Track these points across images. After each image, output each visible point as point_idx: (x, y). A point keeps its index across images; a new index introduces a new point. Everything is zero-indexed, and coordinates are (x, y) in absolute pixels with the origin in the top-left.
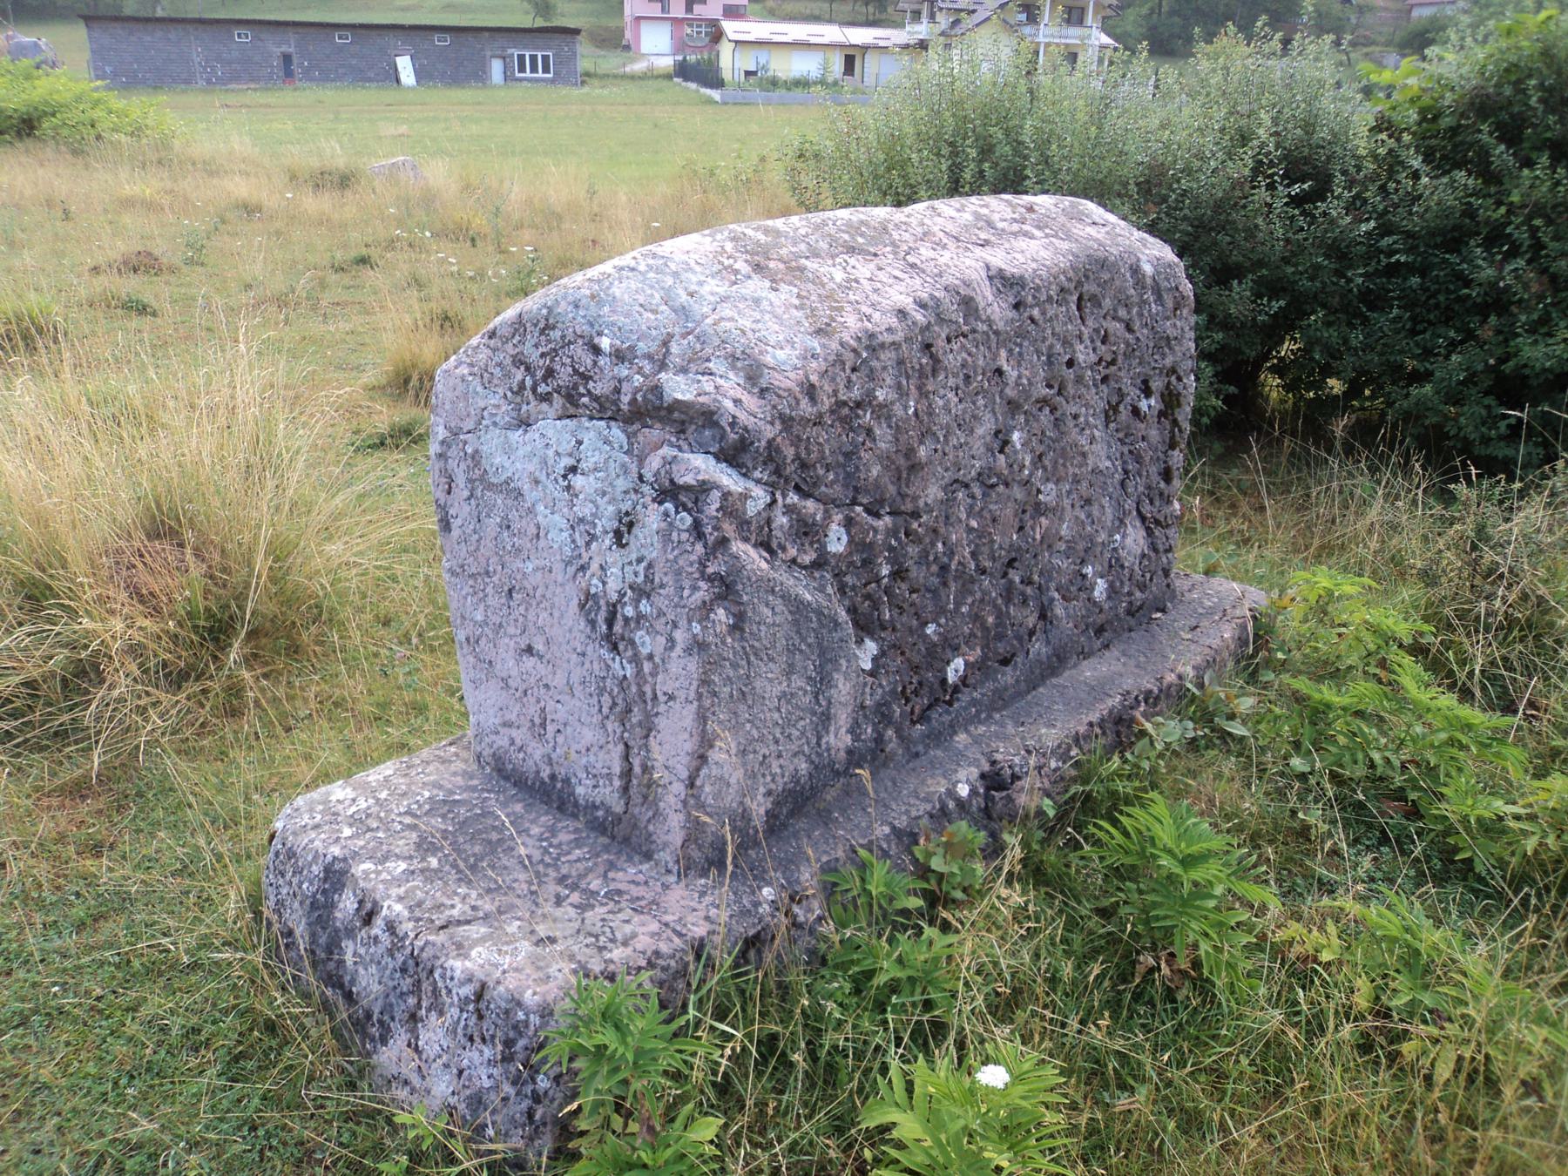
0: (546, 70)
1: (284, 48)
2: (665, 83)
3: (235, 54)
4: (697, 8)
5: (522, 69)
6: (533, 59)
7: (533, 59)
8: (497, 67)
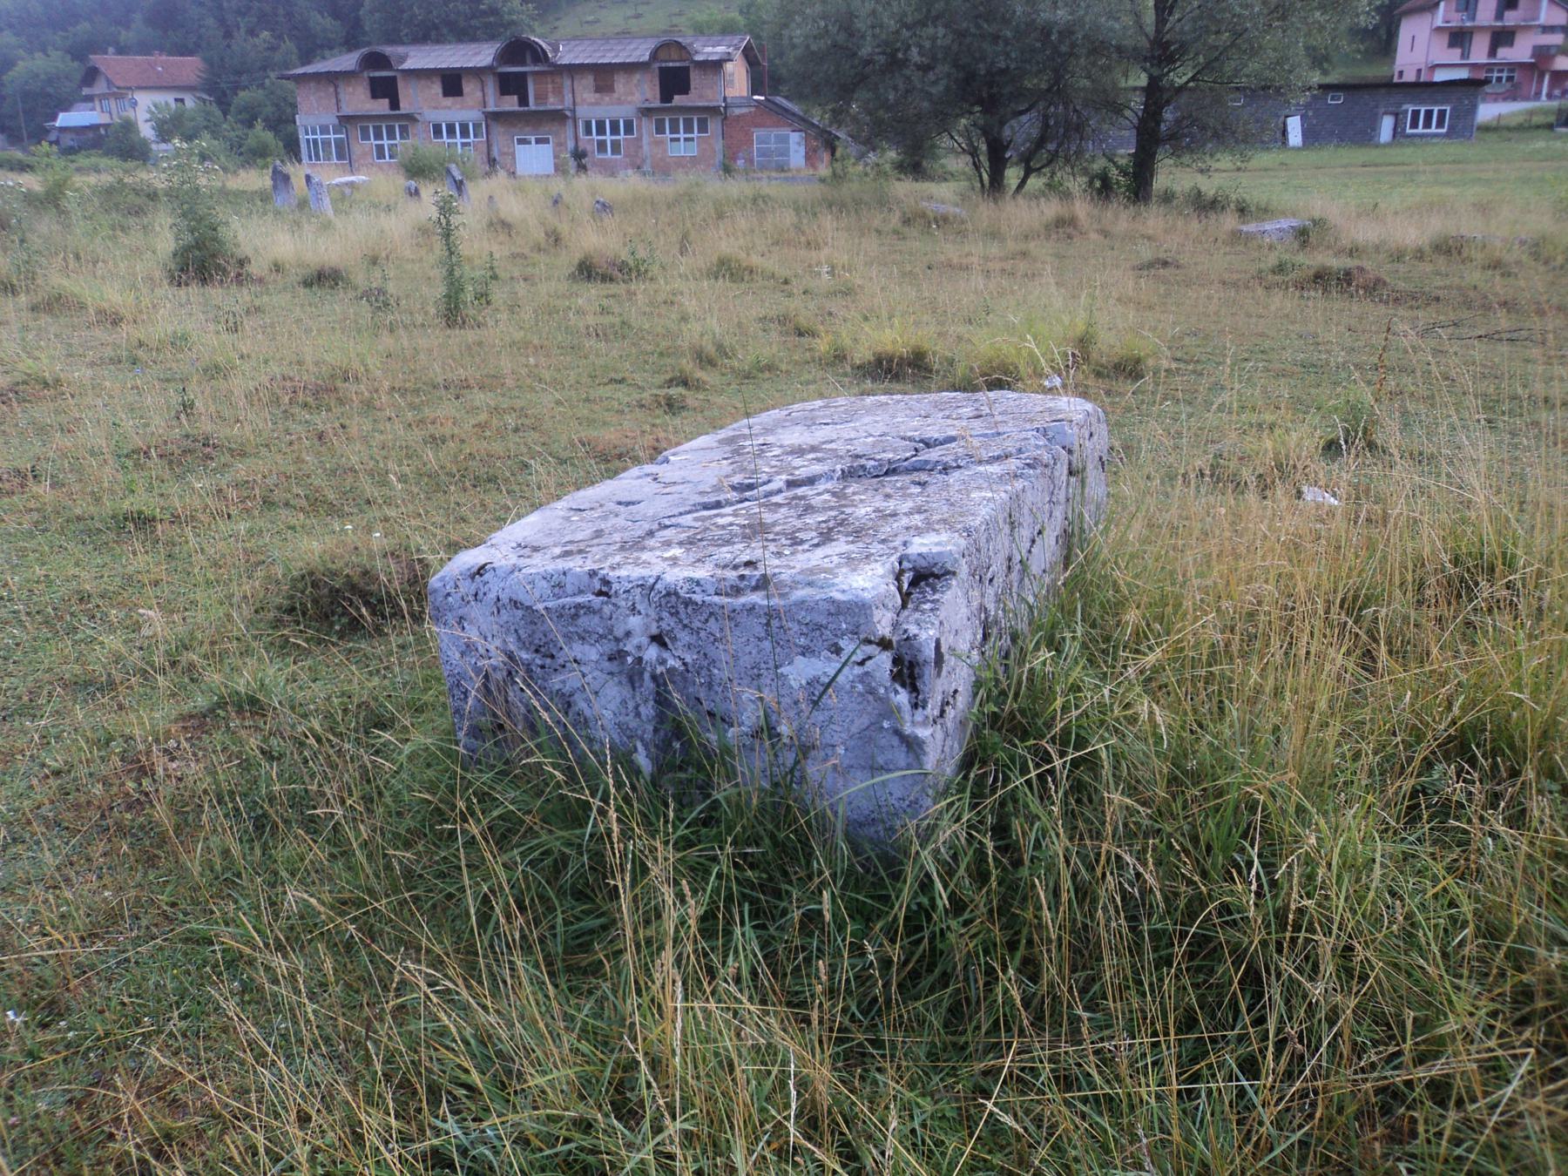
0: (1440, 124)
2: (1546, 132)
4: (1505, 54)
5: (1414, 125)
6: (1429, 114)
7: (1429, 114)
8: (1387, 123)
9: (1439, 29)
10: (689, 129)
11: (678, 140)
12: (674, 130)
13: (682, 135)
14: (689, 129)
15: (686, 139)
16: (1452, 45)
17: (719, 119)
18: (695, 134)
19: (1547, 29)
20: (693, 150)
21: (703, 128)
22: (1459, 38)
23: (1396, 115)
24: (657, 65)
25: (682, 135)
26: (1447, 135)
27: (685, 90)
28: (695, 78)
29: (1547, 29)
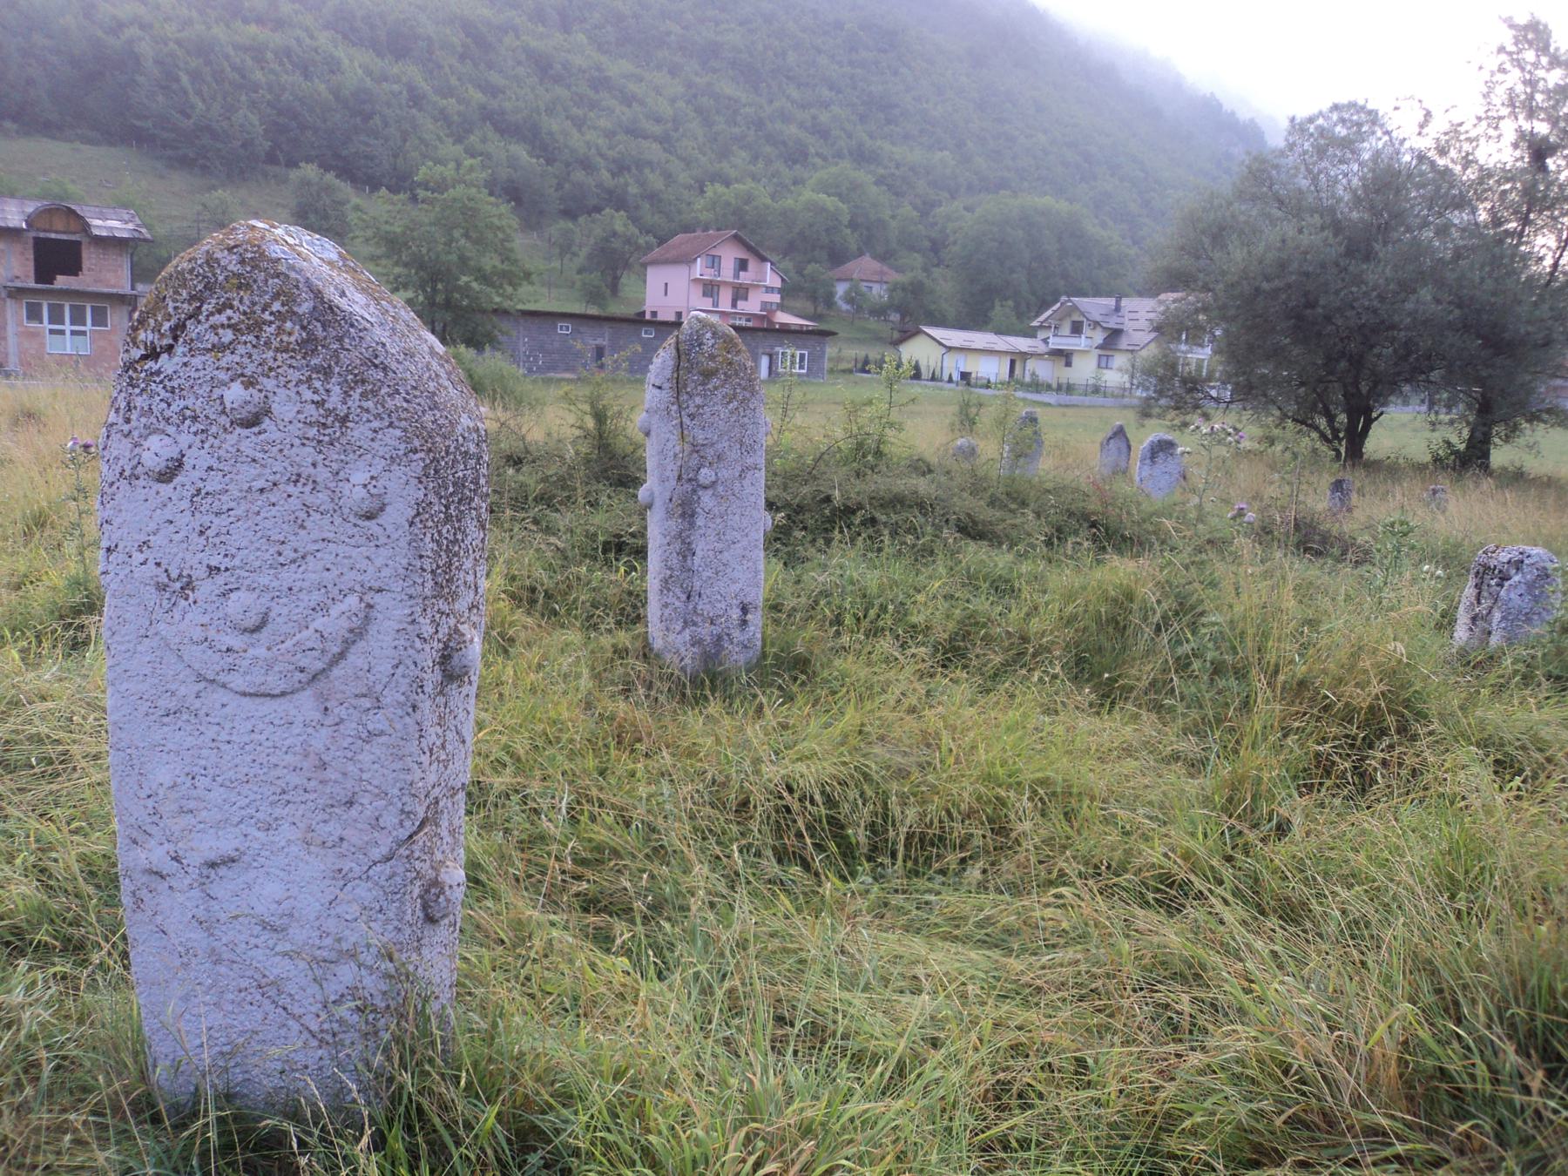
0: (801, 367)
1: (599, 341)
3: (557, 345)
4: (740, 304)
9: (696, 280)
10: (78, 318)
11: (62, 332)
12: (56, 317)
13: (68, 327)
14: (78, 318)
15: (73, 333)
16: (705, 295)
17: (126, 309)
18: (88, 327)
19: (769, 290)
20: (84, 346)
21: (99, 318)
22: (710, 289)
23: (771, 356)
24: (33, 234)
25: (68, 327)
26: (807, 375)
27: (74, 268)
28: (89, 257)
29: (769, 290)
